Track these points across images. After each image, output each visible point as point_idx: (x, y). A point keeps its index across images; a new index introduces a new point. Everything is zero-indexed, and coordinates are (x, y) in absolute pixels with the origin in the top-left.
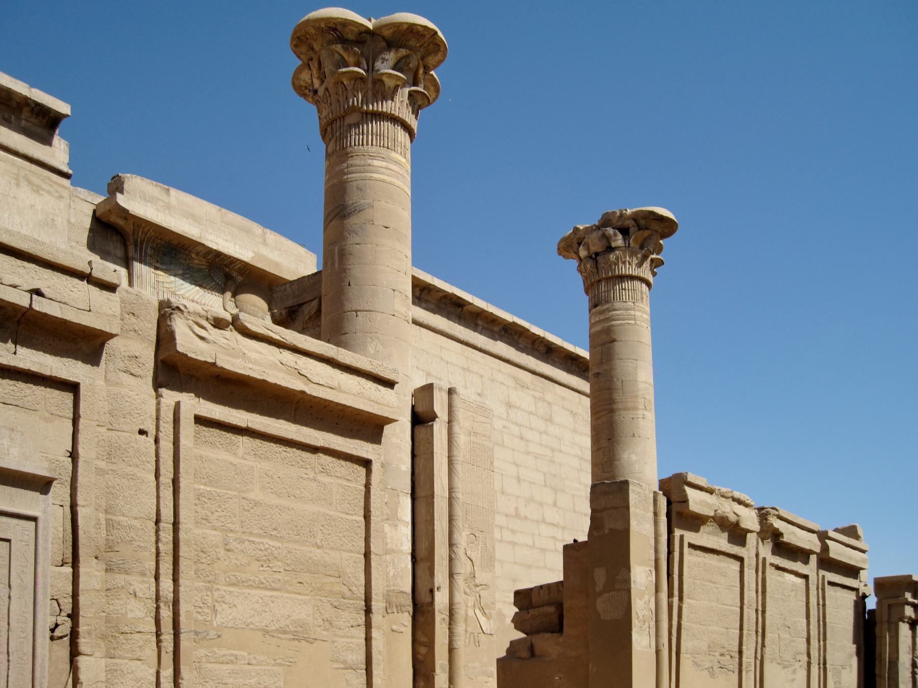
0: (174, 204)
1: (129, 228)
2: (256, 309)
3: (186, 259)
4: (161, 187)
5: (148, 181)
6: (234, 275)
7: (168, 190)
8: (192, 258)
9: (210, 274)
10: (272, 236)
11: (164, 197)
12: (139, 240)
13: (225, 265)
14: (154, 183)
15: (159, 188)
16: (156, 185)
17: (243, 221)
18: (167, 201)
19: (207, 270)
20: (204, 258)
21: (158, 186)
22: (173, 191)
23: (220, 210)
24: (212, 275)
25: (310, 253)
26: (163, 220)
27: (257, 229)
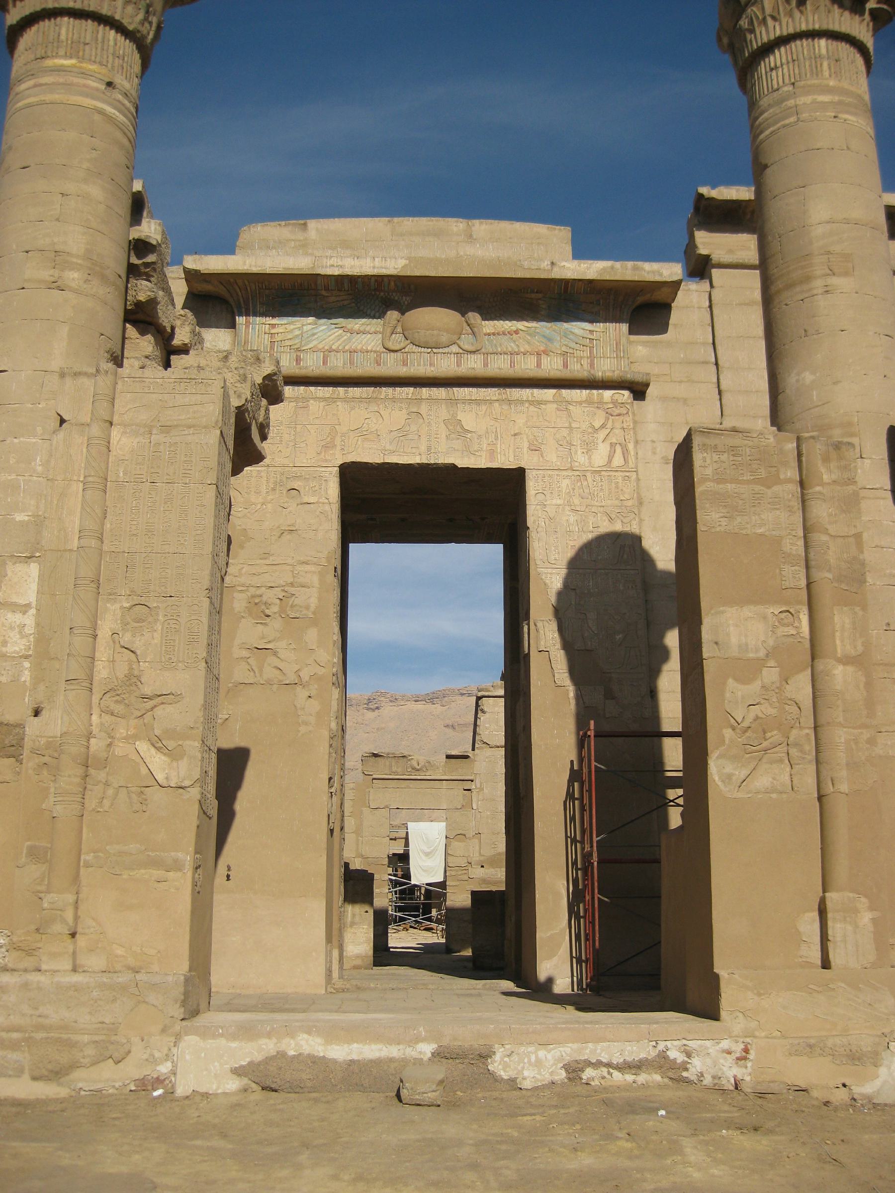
0: (314, 238)
1: (222, 291)
2: (435, 332)
3: (316, 301)
4: (294, 224)
5: (272, 224)
6: (396, 298)
7: (305, 224)
8: (324, 296)
9: (358, 308)
10: (484, 227)
11: (300, 236)
12: (241, 300)
13: (375, 290)
14: (283, 223)
15: (290, 227)
16: (285, 225)
17: (430, 223)
18: (302, 238)
19: (353, 305)
20: (340, 290)
21: (289, 224)
22: (312, 224)
23: (389, 221)
24: (362, 308)
25: (558, 227)
26: (253, 263)
27: (456, 225)
